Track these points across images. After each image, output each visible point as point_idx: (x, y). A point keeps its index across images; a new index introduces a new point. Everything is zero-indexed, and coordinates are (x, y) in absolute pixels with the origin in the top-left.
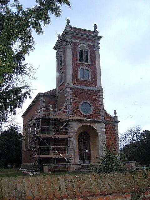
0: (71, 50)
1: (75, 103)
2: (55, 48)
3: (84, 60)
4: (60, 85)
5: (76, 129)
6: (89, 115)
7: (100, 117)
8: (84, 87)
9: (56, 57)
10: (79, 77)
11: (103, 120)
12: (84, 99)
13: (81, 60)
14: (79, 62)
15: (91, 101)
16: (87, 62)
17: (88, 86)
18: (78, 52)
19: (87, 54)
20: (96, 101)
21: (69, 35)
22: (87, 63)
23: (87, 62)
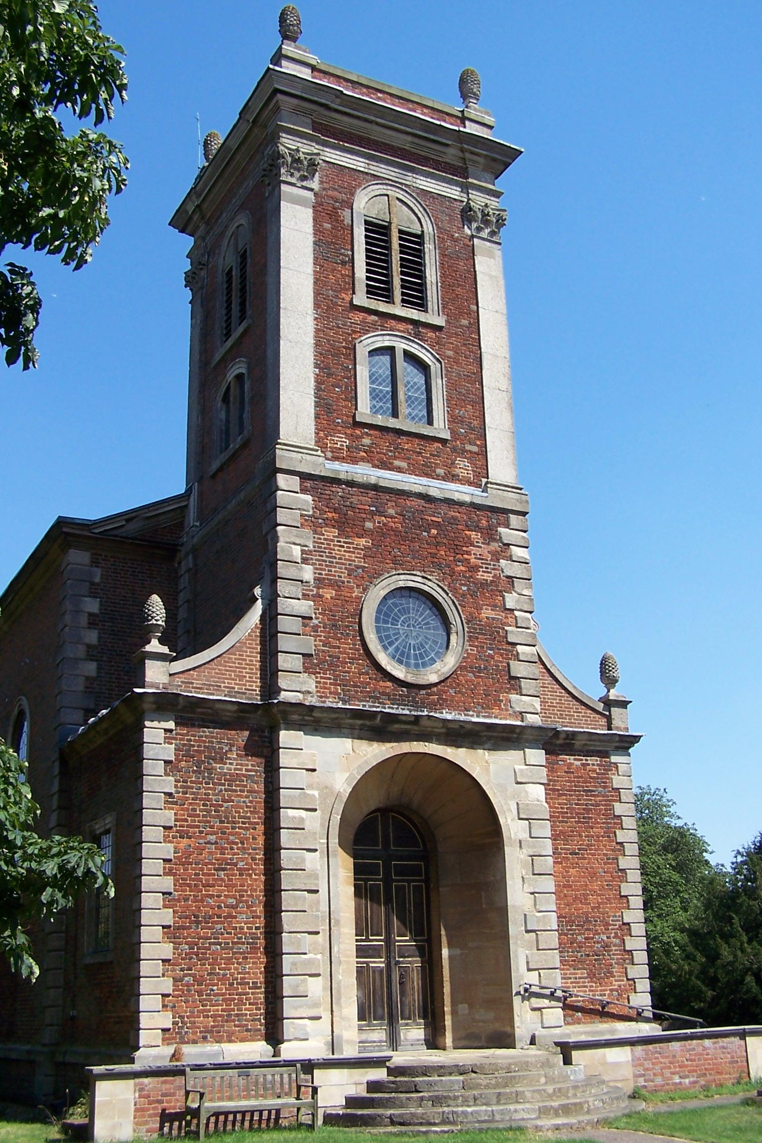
0: (307, 214)
1: (337, 585)
2: (182, 221)
3: (398, 296)
4: (215, 465)
5: (343, 783)
6: (433, 678)
7: (514, 697)
8: (399, 476)
9: (191, 279)
10: (364, 409)
11: (534, 720)
12: (398, 564)
13: (380, 289)
14: (361, 299)
15: (450, 576)
16: (421, 304)
17: (427, 472)
18: (360, 233)
19: (420, 254)
20: (484, 584)
21: (296, 111)
22: (413, 314)
23: (421, 304)
